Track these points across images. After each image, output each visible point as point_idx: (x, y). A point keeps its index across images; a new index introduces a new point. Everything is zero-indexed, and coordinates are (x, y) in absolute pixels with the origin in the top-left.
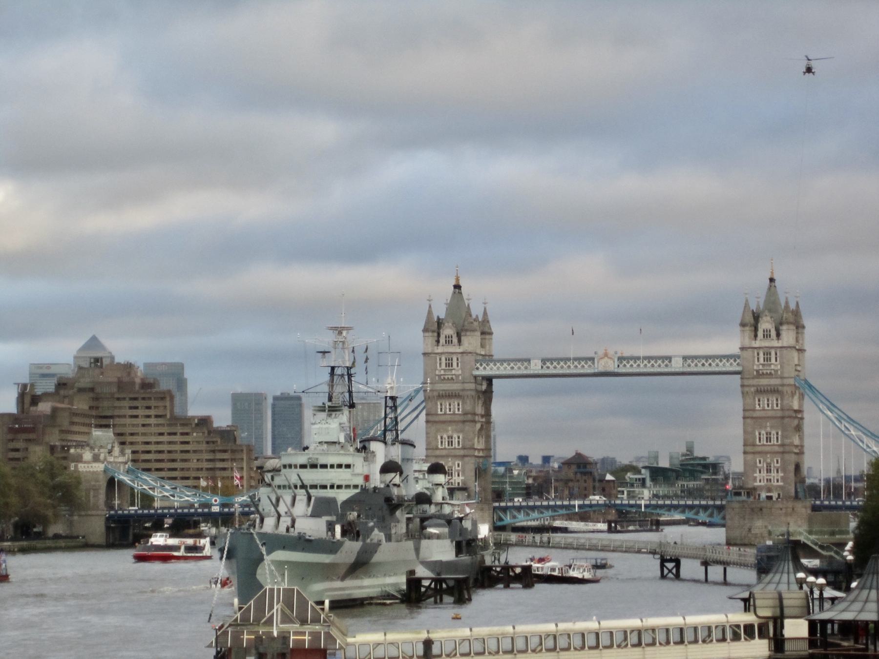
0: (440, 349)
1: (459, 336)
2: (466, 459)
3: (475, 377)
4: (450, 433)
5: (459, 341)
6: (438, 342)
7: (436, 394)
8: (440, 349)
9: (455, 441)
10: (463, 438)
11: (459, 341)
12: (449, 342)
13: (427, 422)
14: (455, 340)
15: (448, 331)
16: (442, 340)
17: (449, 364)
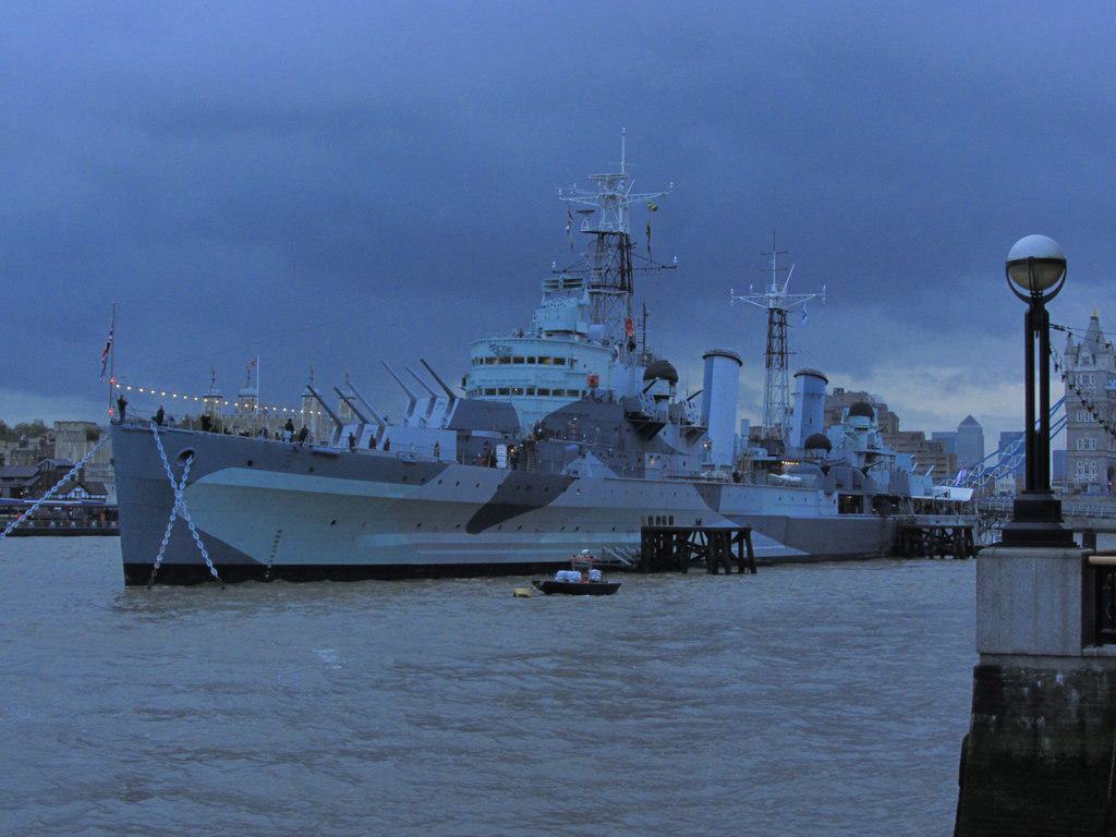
0: (1078, 369)
1: (1094, 357)
2: (1100, 459)
3: (1108, 392)
4: (1087, 438)
5: (1094, 362)
6: (1077, 362)
7: (1075, 405)
8: (1078, 369)
9: (1091, 444)
10: (1098, 442)
11: (1094, 362)
12: (1086, 362)
13: (1068, 428)
14: (1091, 361)
15: (1085, 354)
16: (1080, 362)
17: (1086, 379)
